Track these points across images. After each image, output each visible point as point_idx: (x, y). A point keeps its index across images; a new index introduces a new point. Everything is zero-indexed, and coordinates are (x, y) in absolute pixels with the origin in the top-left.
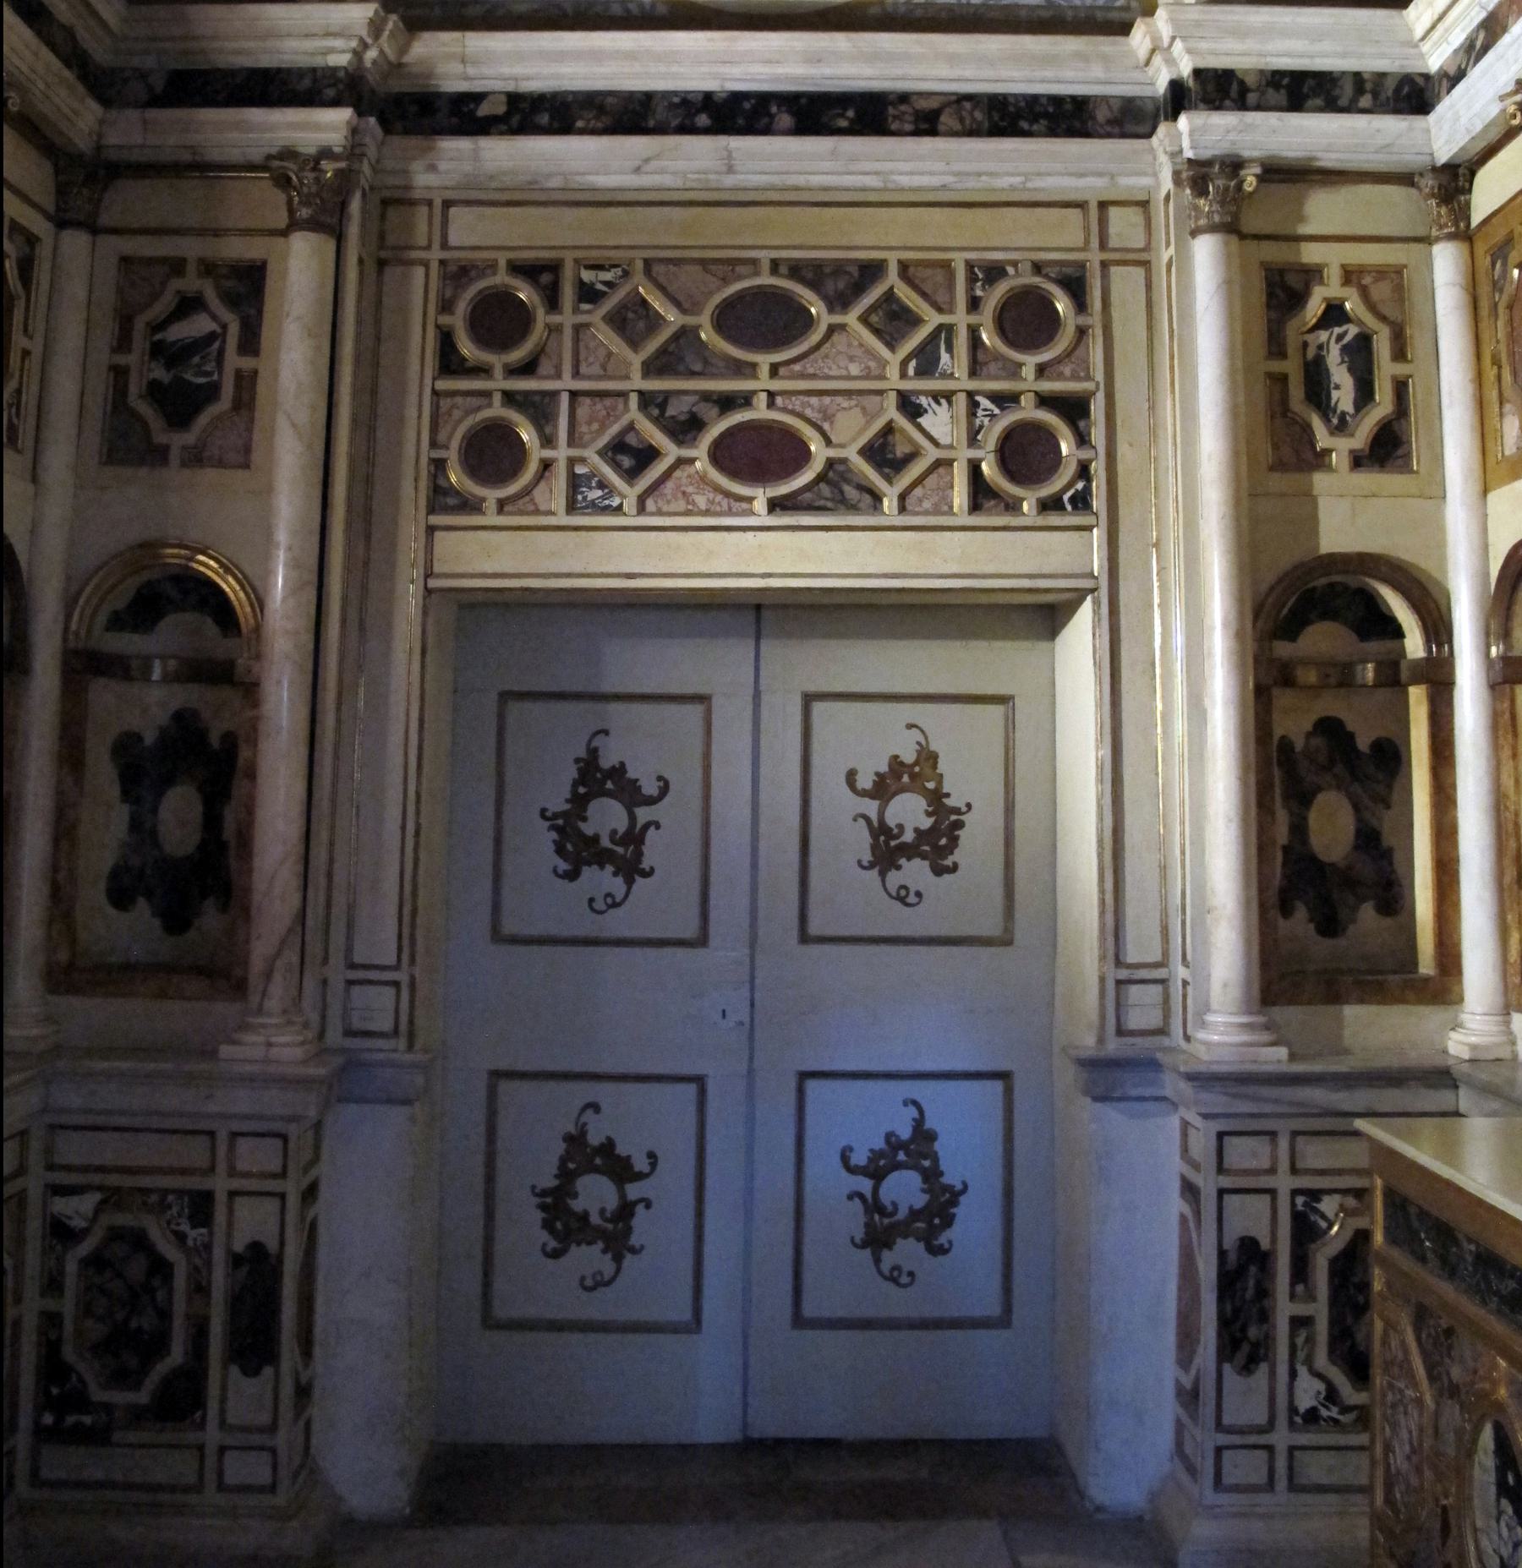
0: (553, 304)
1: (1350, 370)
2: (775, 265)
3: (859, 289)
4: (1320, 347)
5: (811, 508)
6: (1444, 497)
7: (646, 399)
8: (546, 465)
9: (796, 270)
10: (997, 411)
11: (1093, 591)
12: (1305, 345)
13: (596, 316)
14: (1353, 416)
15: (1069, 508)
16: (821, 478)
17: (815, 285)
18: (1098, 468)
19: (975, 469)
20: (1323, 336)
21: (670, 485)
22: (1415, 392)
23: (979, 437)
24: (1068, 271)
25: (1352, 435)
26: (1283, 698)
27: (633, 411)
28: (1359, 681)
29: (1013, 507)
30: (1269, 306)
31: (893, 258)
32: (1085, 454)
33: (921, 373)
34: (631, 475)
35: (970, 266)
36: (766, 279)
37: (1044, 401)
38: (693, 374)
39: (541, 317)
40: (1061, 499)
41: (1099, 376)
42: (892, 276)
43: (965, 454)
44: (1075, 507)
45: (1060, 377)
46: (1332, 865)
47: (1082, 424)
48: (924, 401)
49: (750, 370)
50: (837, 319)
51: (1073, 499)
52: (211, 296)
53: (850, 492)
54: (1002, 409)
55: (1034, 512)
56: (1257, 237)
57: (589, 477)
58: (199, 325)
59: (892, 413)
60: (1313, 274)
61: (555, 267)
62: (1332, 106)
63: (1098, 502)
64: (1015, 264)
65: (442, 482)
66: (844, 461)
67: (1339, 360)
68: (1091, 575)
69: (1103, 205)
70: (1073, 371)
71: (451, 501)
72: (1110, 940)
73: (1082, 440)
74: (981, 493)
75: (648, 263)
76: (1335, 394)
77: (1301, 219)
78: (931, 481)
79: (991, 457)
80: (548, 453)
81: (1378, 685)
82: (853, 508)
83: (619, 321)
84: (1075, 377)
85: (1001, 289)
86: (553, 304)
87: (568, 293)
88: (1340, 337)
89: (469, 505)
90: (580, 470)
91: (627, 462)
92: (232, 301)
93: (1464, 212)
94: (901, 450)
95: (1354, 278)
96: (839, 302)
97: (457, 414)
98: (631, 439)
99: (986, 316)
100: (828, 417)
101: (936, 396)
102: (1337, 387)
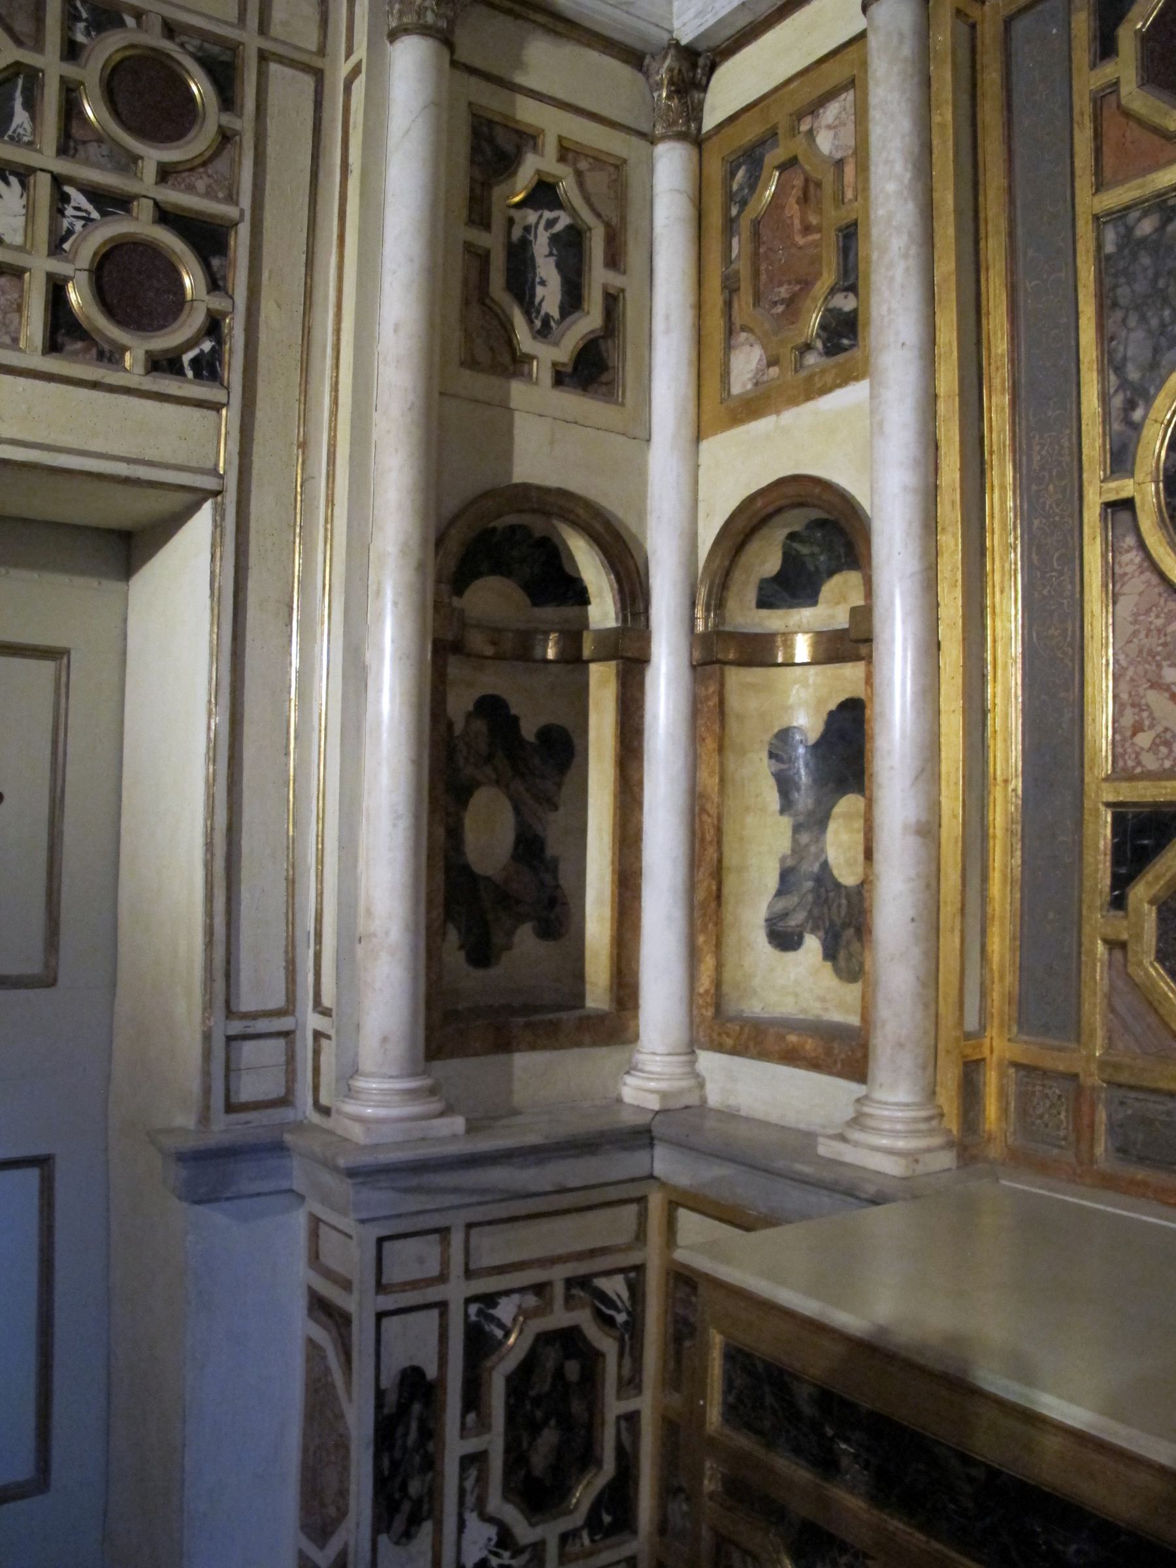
1: (558, 266)
4: (527, 229)
6: (649, 440)
10: (95, 215)
11: (217, 493)
12: (511, 221)
14: (559, 323)
15: (190, 374)
18: (235, 328)
19: (56, 290)
20: (531, 217)
23: (66, 246)
24: (216, 50)
25: (556, 344)
26: (455, 668)
28: (538, 653)
29: (110, 356)
30: (472, 162)
32: (217, 303)
37: (165, 216)
40: (179, 359)
41: (246, 201)
43: (41, 265)
44: (198, 375)
45: (191, 189)
46: (488, 879)
47: (215, 262)
51: (195, 362)
54: (104, 214)
55: (140, 369)
56: (472, 71)
60: (527, 138)
63: (234, 374)
64: (138, 14)
67: (547, 251)
68: (214, 472)
70: (209, 186)
72: (220, 985)
73: (215, 284)
76: (540, 291)
77: (518, 63)
79: (83, 277)
81: (560, 660)
84: (209, 194)
88: (551, 224)
93: (695, 113)
95: (570, 156)
99: (91, 73)
102: (543, 283)
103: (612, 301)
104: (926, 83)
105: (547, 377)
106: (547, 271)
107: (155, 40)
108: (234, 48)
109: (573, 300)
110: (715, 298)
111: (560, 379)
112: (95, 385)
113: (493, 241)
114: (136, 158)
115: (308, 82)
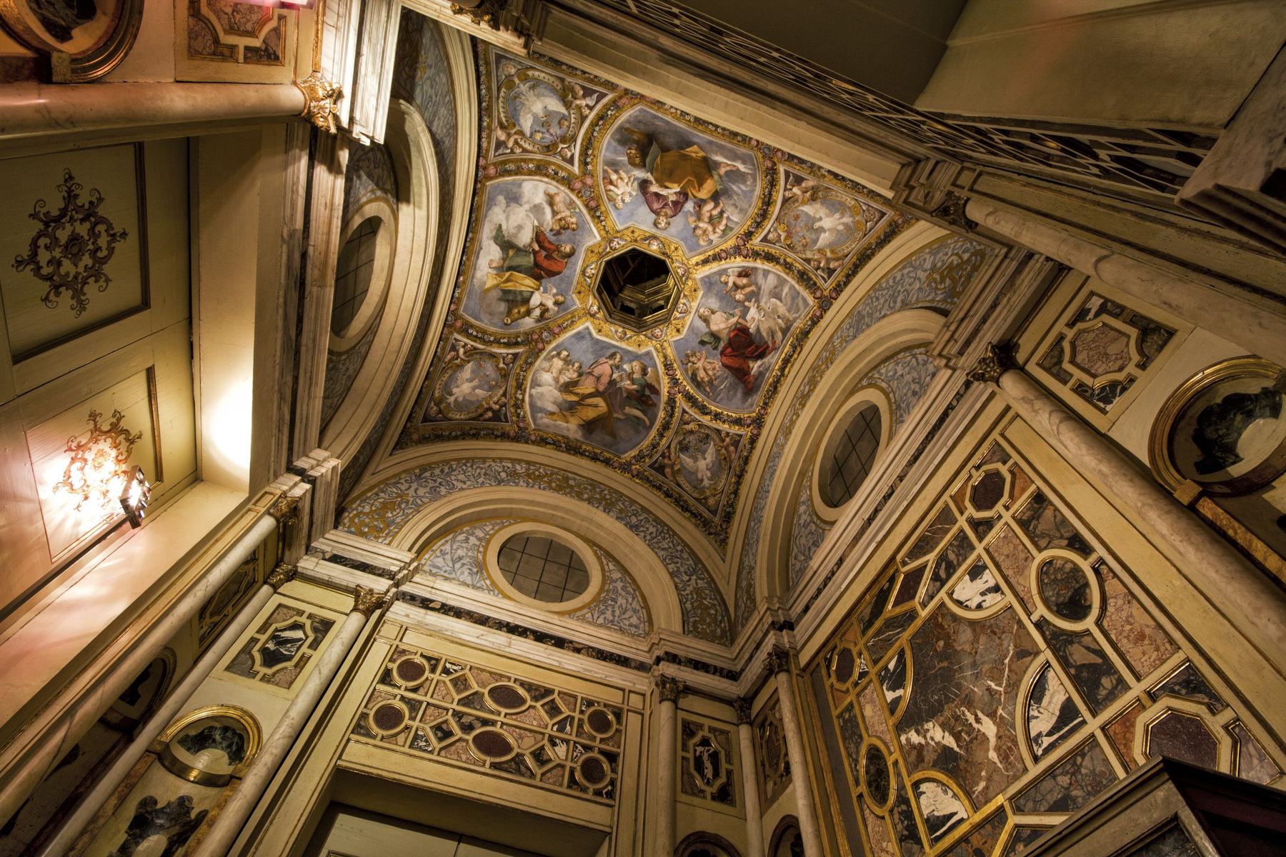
0: (433, 670)
2: (516, 680)
3: (543, 696)
5: (506, 771)
7: (457, 714)
8: (407, 728)
9: (522, 684)
12: (695, 751)
13: (447, 679)
16: (513, 759)
17: (529, 690)
21: (453, 748)
22: (735, 777)
27: (449, 717)
31: (557, 690)
32: (614, 776)
33: (558, 730)
34: (440, 740)
35: (582, 699)
36: (511, 684)
37: (602, 752)
38: (476, 709)
39: (427, 674)
41: (622, 747)
42: (556, 695)
43: (569, 764)
48: (557, 741)
49: (499, 714)
50: (533, 704)
51: (606, 793)
52: (308, 628)
53: (523, 768)
57: (422, 737)
58: (298, 634)
59: (546, 742)
61: (438, 660)
62: (707, 672)
64: (598, 703)
65: (362, 723)
66: (523, 755)
69: (630, 691)
71: (362, 731)
73: (614, 771)
74: (573, 782)
75: (471, 667)
78: (554, 772)
80: (411, 723)
82: (523, 775)
83: (455, 682)
85: (592, 709)
86: (433, 670)
87: (440, 669)
89: (368, 734)
90: (420, 733)
91: (440, 734)
92: (315, 630)
94: (545, 758)
96: (536, 699)
97: (380, 699)
98: (444, 726)
99: (585, 717)
100: (522, 738)
101: (563, 740)
103: (729, 773)
104: (793, 693)
105: (709, 797)
106: (708, 764)
107: (602, 708)
108: (621, 709)
109: (716, 774)
110: (760, 769)
111: (714, 798)
112: (579, 798)
113: (690, 756)
114: (595, 737)
115: (640, 717)
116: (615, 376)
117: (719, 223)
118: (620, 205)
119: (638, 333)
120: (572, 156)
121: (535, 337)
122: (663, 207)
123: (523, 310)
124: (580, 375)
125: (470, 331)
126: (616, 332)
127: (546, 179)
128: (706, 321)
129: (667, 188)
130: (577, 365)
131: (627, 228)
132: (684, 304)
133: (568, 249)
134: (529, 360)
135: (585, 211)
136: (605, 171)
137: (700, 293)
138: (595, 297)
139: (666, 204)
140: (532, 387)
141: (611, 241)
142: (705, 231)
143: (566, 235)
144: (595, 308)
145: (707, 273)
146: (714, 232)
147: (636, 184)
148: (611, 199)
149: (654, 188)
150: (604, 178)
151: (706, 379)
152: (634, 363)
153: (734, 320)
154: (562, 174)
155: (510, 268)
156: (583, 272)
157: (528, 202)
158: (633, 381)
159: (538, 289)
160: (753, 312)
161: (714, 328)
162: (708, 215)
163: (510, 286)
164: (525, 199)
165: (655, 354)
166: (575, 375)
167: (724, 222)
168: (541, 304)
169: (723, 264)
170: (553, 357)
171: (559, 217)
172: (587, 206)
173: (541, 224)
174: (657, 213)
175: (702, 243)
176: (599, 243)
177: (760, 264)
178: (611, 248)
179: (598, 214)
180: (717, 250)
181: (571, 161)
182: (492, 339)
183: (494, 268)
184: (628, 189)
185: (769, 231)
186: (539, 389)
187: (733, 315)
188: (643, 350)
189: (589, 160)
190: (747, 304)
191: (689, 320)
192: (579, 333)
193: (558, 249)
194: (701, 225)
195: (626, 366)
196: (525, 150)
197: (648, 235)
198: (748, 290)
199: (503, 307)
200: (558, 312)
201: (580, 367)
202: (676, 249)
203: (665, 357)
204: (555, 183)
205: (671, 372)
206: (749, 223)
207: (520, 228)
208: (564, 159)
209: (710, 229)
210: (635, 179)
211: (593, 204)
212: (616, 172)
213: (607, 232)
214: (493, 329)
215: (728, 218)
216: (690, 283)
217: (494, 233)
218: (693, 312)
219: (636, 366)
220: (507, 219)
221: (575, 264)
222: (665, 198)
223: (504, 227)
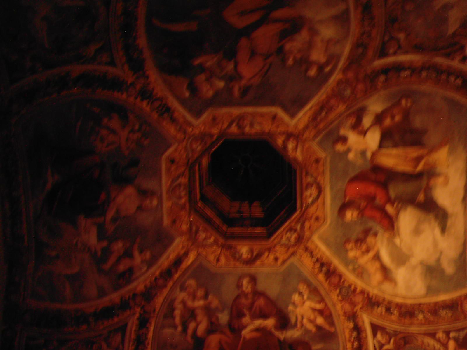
116: (231, 66)
117: (182, 316)
118: (302, 288)
119: (222, 134)
120: (375, 335)
121: (360, 87)
122: (253, 303)
123: (388, 122)
124: (280, 50)
125: (459, 82)
126: (252, 125)
127: (399, 300)
128: (144, 194)
129: (257, 330)
130: (290, 62)
131: (284, 261)
132: (180, 198)
133: (350, 215)
134: (360, 50)
135: (341, 268)
136: (332, 324)
137: (166, 221)
138: (295, 159)
139: (250, 308)
140: (347, 12)
141: (300, 239)
142: (194, 297)
143: (357, 232)
144: (290, 146)
145: (171, 248)
146: (183, 302)
147: (293, 320)
148: (314, 291)
149: (270, 323)
150: (331, 315)
151: (105, 121)
152: (211, 93)
153: (110, 214)
154: (381, 310)
155: (419, 176)
156: (320, 190)
157: (414, 268)
158: (202, 68)
159: (374, 154)
160: (92, 239)
161: (130, 190)
162: (199, 318)
163: (413, 152)
164: (419, 271)
165: (189, 117)
166: (288, 47)
167: (177, 320)
168: (364, 133)
169: (156, 270)
170: (327, 63)
171: (371, 254)
172: (340, 276)
173: (391, 242)
174: (257, 294)
175: (192, 282)
176: (312, 234)
177: (115, 297)
178: (295, 230)
179: (324, 269)
180: (171, 284)
181: (375, 328)
182: (424, 74)
183: (439, 175)
184: (299, 311)
185: (123, 341)
186: (333, 11)
187: (114, 219)
188: (205, 116)
189: (355, 334)
190: (105, 244)
191: (165, 182)
192: (302, 105)
193: (362, 213)
194: (201, 303)
195: (221, 84)
196: (433, 335)
197: (258, 262)
198: (112, 260)
199: (418, 122)
200: (338, 127)
201: (284, 61)
202: (218, 260)
203: (173, 120)
204: (388, 297)
205: (157, 104)
206: (150, 335)
207: (417, 232)
208: (383, 329)
209: (190, 303)
210: (296, 325)
211: (335, 280)
212: (319, 328)
213: (306, 249)
214: (427, 87)
215: (175, 327)
216: (185, 227)
217: (449, 223)
218: (165, 196)
219: (208, 92)
220: (435, 244)
221: (333, 199)
222: (254, 317)
223: (437, 231)
